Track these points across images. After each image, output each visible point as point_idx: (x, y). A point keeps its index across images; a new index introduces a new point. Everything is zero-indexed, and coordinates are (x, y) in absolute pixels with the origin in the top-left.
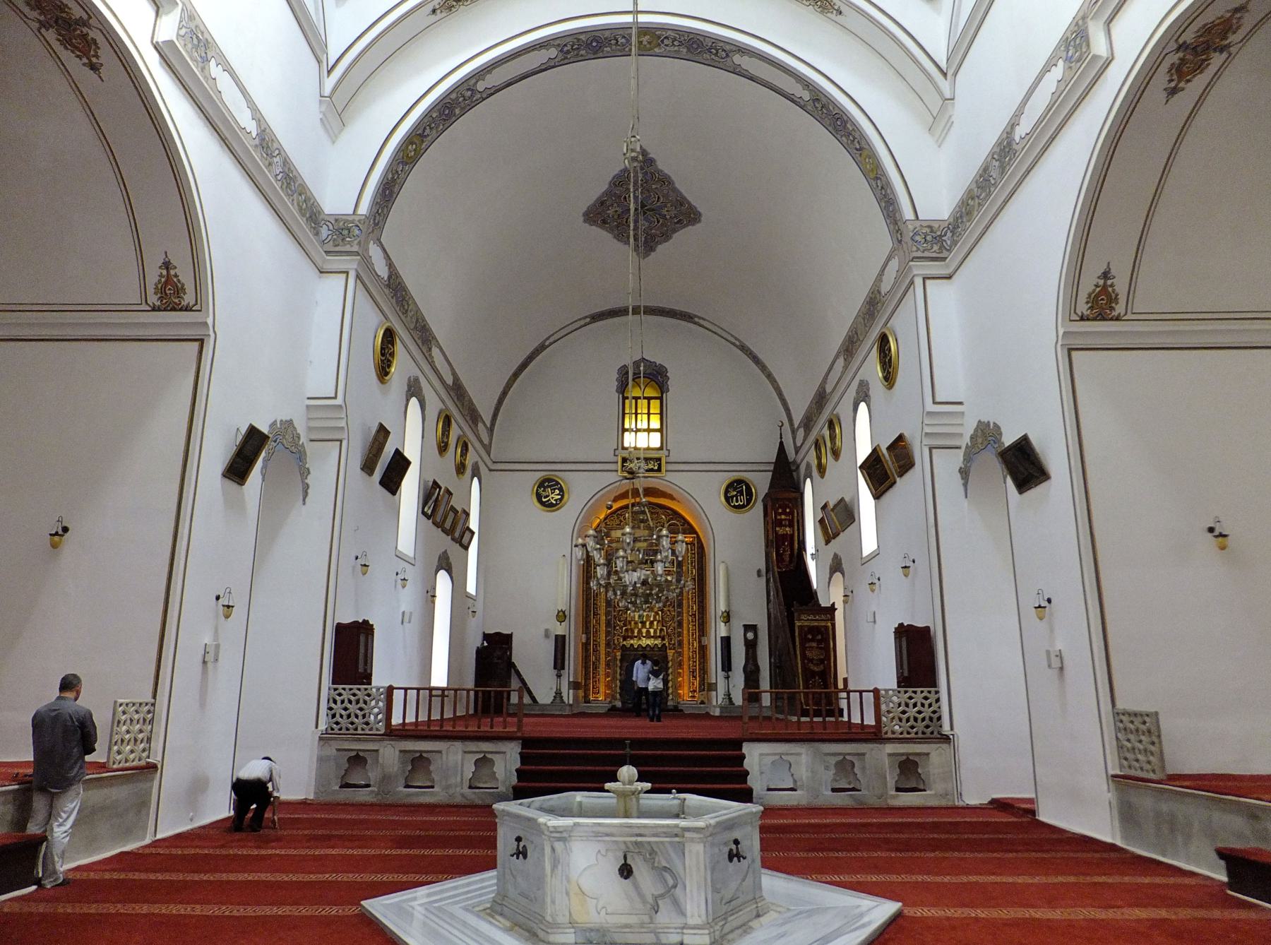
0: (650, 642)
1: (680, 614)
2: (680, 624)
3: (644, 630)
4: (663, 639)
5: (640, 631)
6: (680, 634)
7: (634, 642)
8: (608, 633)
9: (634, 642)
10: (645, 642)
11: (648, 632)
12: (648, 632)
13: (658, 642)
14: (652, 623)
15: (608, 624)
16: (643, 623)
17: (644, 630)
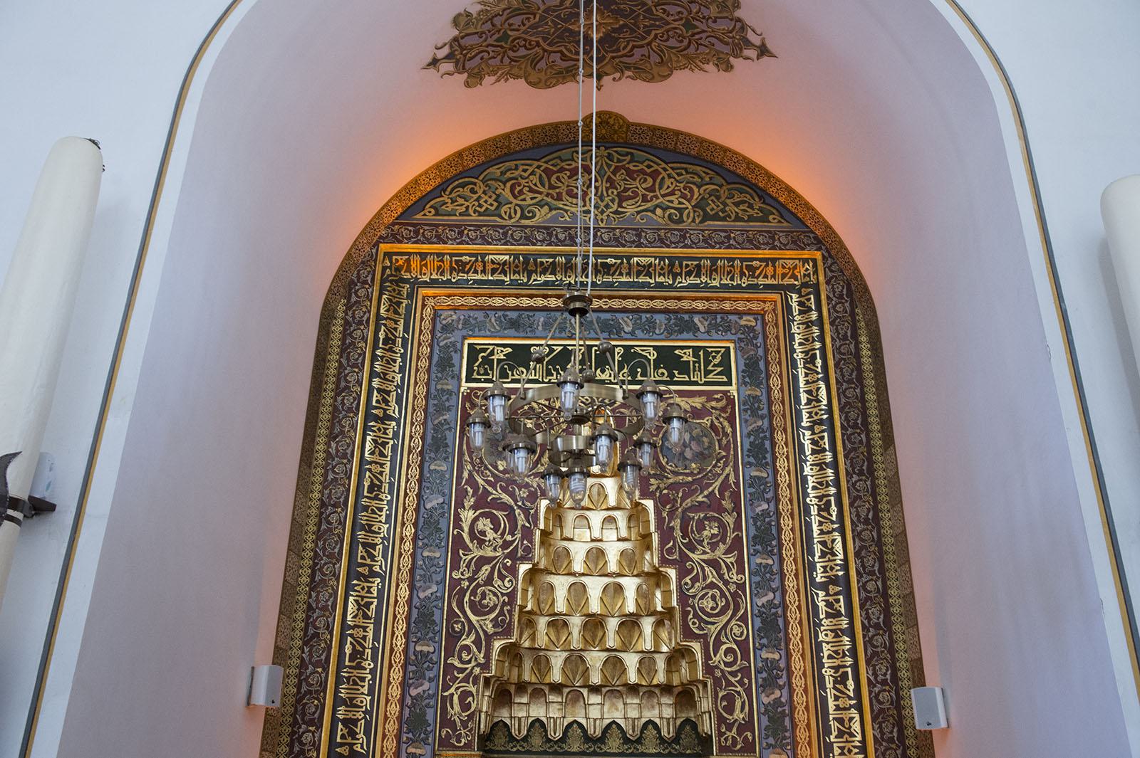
0: (626, 713)
1: (768, 578)
2: (772, 626)
3: (595, 659)
4: (685, 696)
5: (575, 660)
6: (773, 676)
7: (551, 712)
8: (415, 666)
9: (551, 712)
10: (597, 713)
11: (614, 663)
12: (614, 663)
13: (663, 712)
14: (630, 624)
15: (421, 620)
16: (594, 624)
17: (595, 659)
